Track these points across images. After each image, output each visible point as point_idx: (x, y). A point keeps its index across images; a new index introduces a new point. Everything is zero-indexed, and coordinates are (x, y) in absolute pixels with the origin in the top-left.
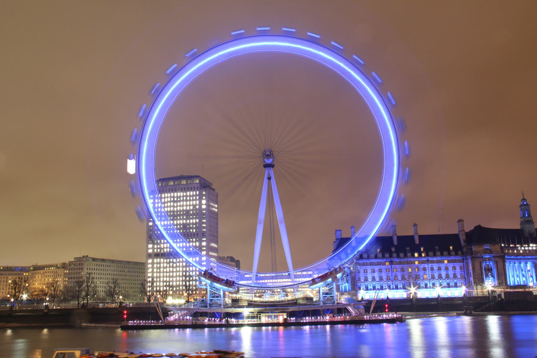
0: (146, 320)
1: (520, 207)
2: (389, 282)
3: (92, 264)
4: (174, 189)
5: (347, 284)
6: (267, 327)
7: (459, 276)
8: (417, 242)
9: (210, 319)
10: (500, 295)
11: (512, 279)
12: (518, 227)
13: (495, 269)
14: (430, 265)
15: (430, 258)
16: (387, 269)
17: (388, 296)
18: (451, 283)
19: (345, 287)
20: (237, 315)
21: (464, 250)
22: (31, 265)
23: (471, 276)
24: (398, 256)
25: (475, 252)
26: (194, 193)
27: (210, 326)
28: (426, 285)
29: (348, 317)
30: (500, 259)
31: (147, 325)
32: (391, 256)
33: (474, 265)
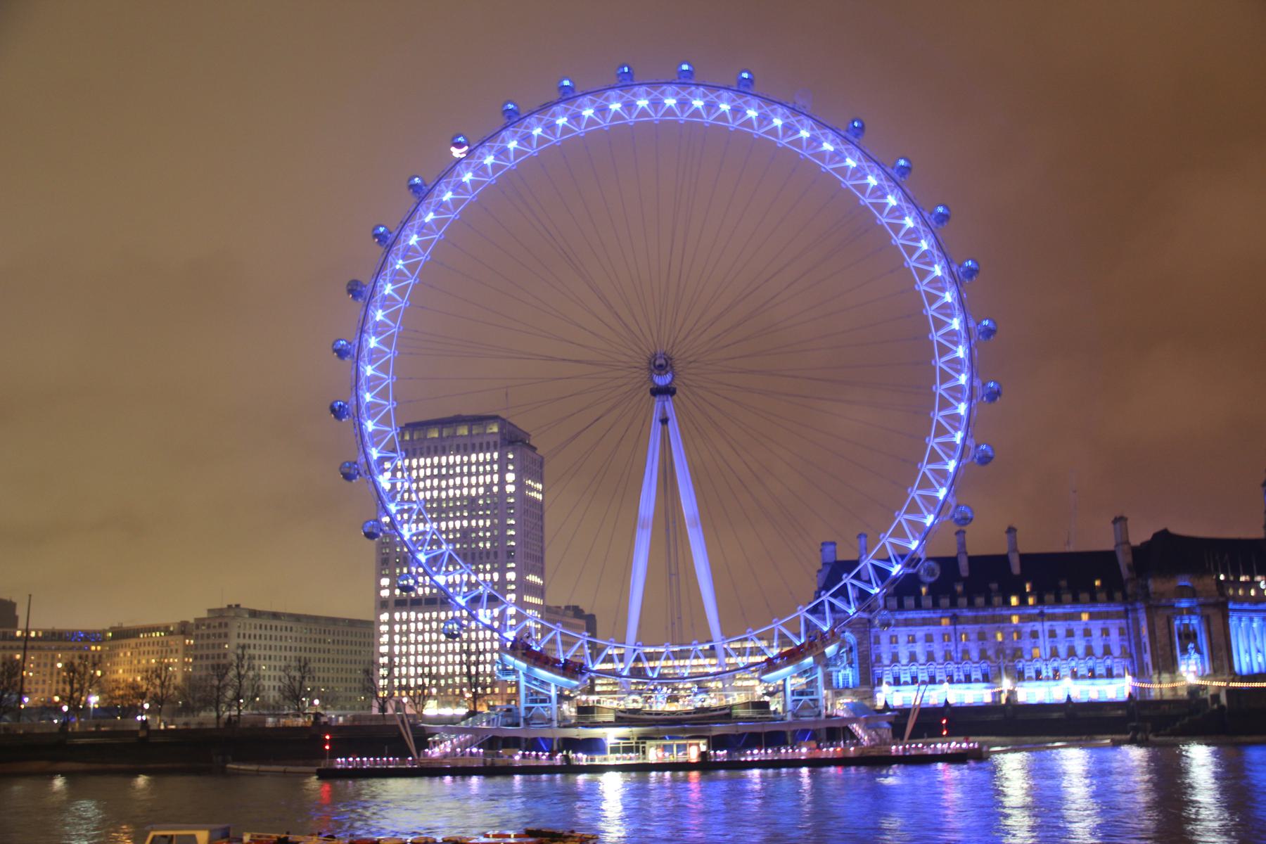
0: (375, 757)
2: (949, 666)
3: (250, 624)
4: (439, 448)
5: (849, 671)
6: (660, 773)
7: (1116, 652)
8: (1016, 569)
9: (527, 753)
10: (1216, 697)
11: (1245, 659)
14: (1047, 625)
16: (944, 635)
17: (946, 700)
19: (846, 678)
20: (593, 746)
21: (1129, 588)
22: (107, 628)
24: (971, 605)
25: (1155, 593)
26: (488, 456)
27: (524, 770)
28: (1038, 673)
29: (852, 749)
31: (378, 767)
32: (954, 604)
33: (1153, 624)
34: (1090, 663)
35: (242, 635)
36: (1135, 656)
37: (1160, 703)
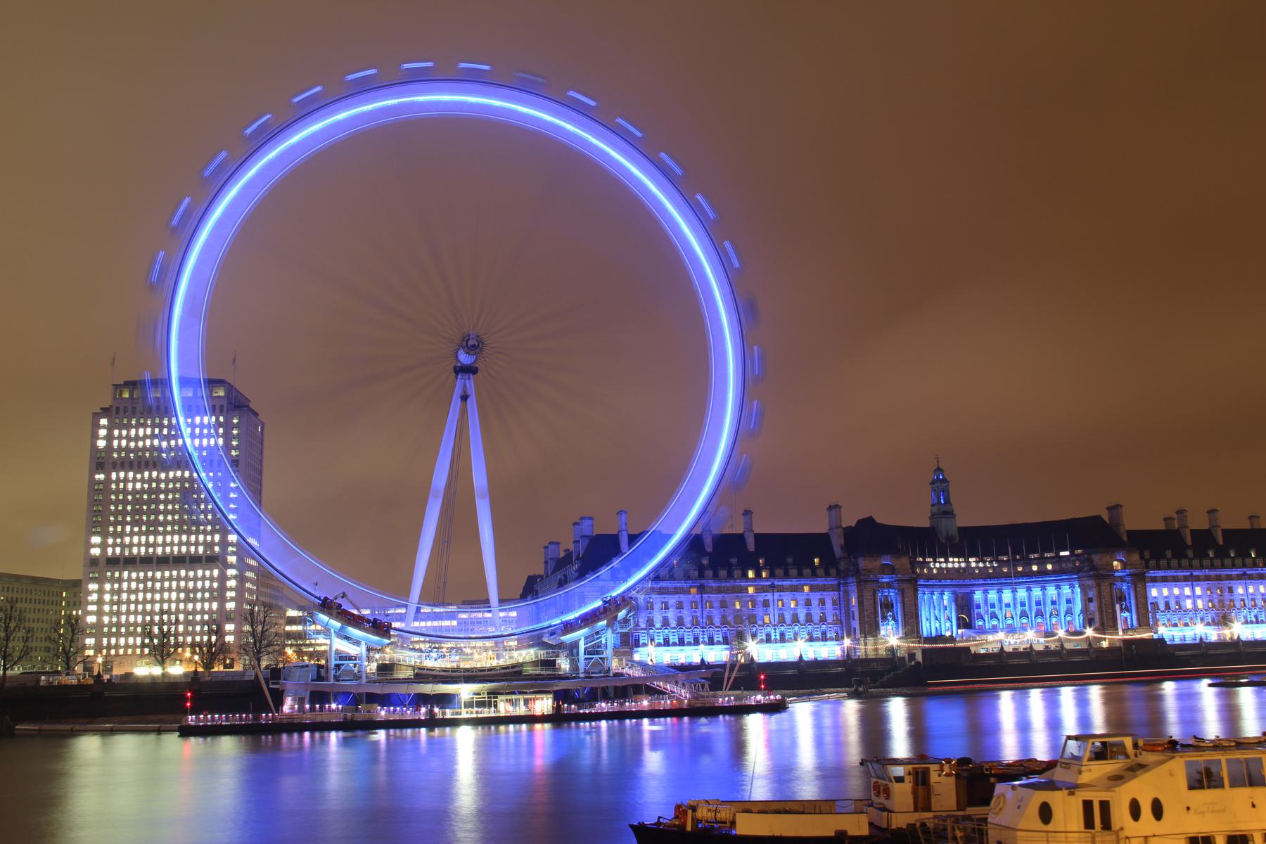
0: (241, 714)
1: (930, 484)
2: (696, 629)
6: (518, 726)
10: (912, 656)
12: (926, 523)
13: (899, 605)
14: (777, 595)
15: (778, 581)
20: (445, 700)
21: (842, 566)
23: (854, 619)
24: (716, 576)
25: (864, 570)
27: (386, 725)
30: (909, 585)
31: (201, 724)
33: (863, 596)
36: (844, 624)
37: (866, 661)
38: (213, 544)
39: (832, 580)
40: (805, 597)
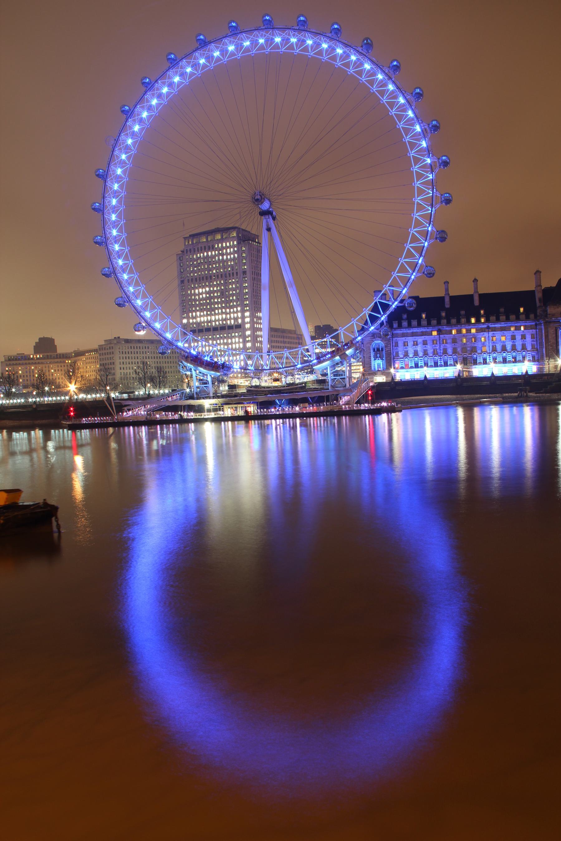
2: (435, 357)
3: (125, 347)
4: (207, 247)
5: (379, 362)
7: (529, 348)
8: (477, 302)
9: (167, 413)
14: (491, 333)
15: (491, 324)
16: (433, 341)
18: (518, 357)
21: (539, 311)
22: (72, 351)
25: (549, 314)
28: (515, 358)
29: (322, 407)
33: (548, 332)
34: (514, 354)
35: (124, 353)
38: (238, 318)
39: (530, 322)
40: (511, 334)
